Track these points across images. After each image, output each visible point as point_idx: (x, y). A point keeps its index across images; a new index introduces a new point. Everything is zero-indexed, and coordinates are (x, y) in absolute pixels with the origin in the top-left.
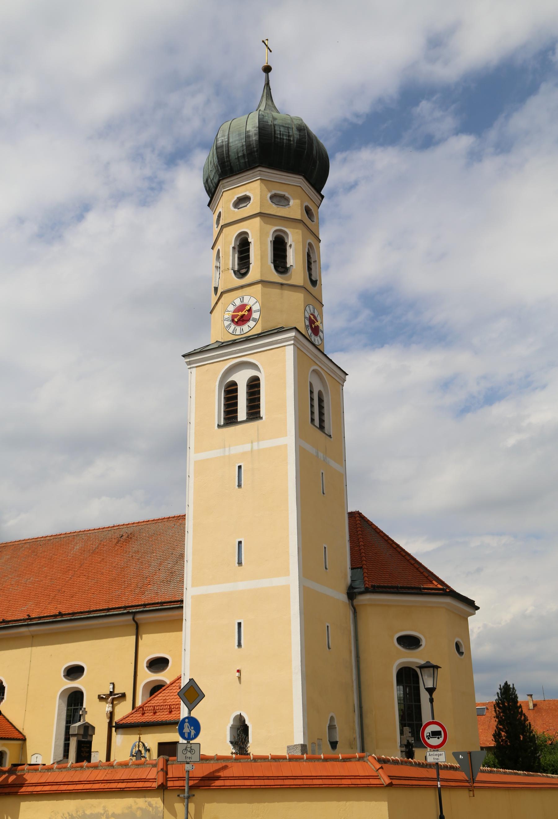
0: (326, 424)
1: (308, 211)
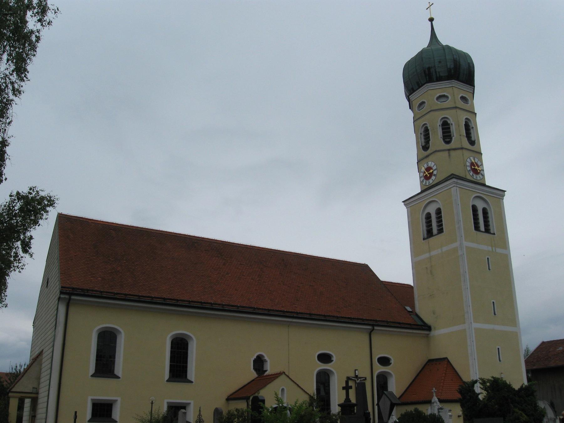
0: (491, 227)
1: (463, 98)
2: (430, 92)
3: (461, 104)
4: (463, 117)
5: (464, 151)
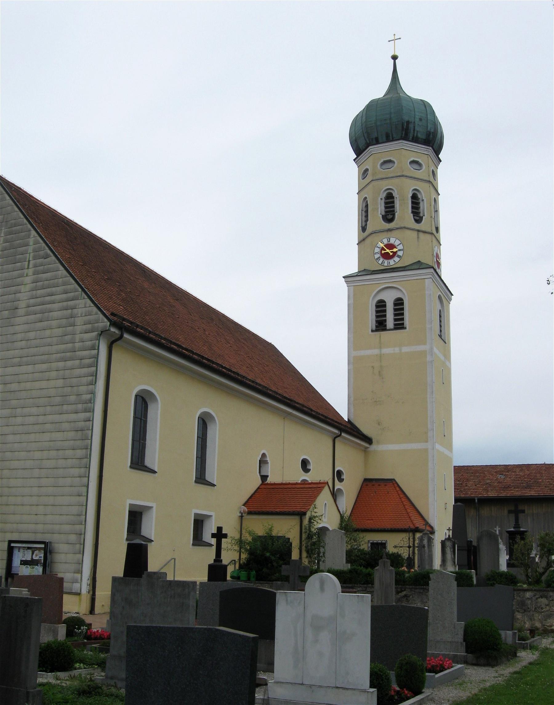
2: (404, 152)
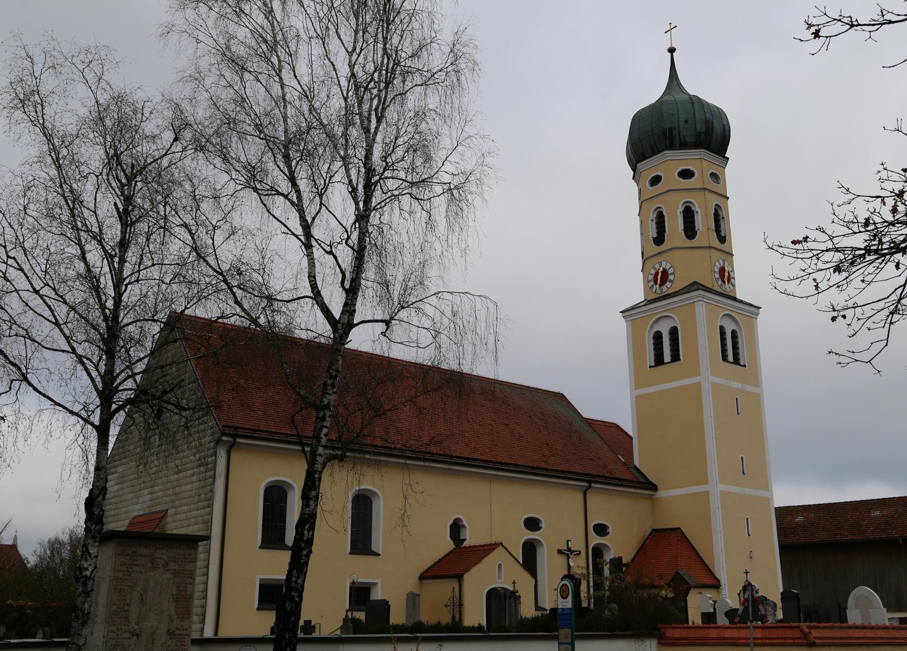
1: (714, 176)
2: (669, 163)
3: (710, 184)
4: (714, 201)
5: (712, 251)
